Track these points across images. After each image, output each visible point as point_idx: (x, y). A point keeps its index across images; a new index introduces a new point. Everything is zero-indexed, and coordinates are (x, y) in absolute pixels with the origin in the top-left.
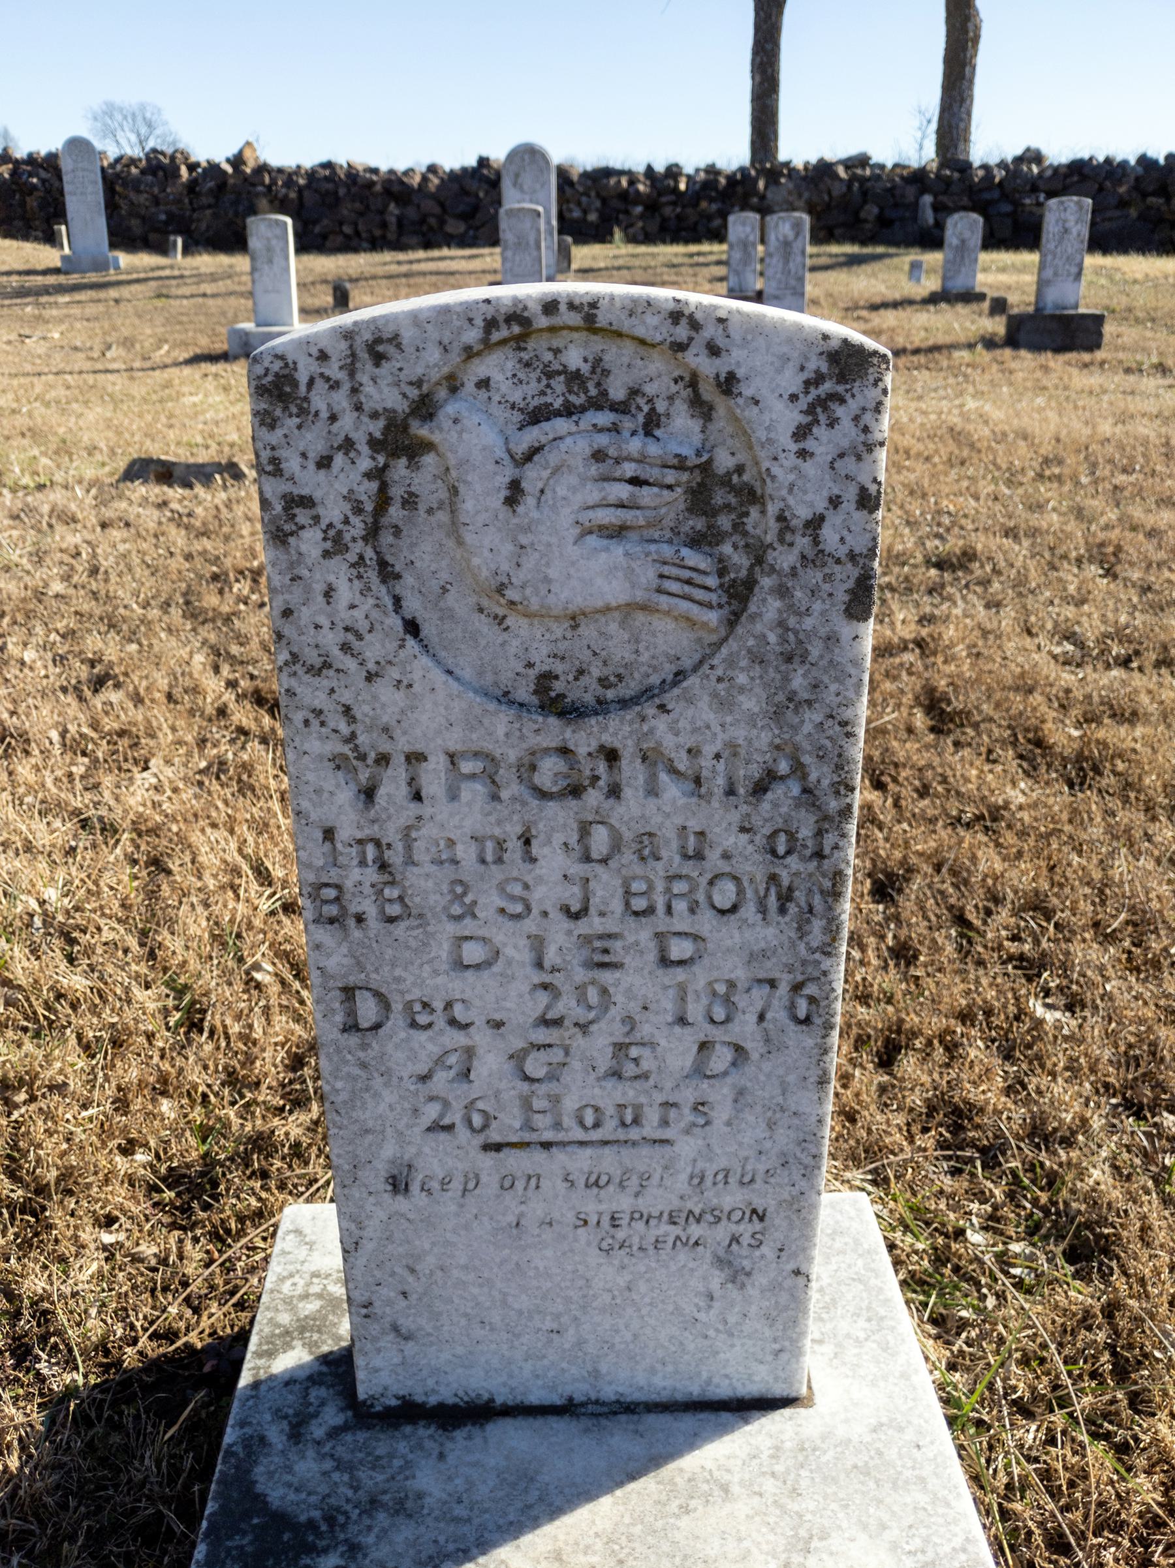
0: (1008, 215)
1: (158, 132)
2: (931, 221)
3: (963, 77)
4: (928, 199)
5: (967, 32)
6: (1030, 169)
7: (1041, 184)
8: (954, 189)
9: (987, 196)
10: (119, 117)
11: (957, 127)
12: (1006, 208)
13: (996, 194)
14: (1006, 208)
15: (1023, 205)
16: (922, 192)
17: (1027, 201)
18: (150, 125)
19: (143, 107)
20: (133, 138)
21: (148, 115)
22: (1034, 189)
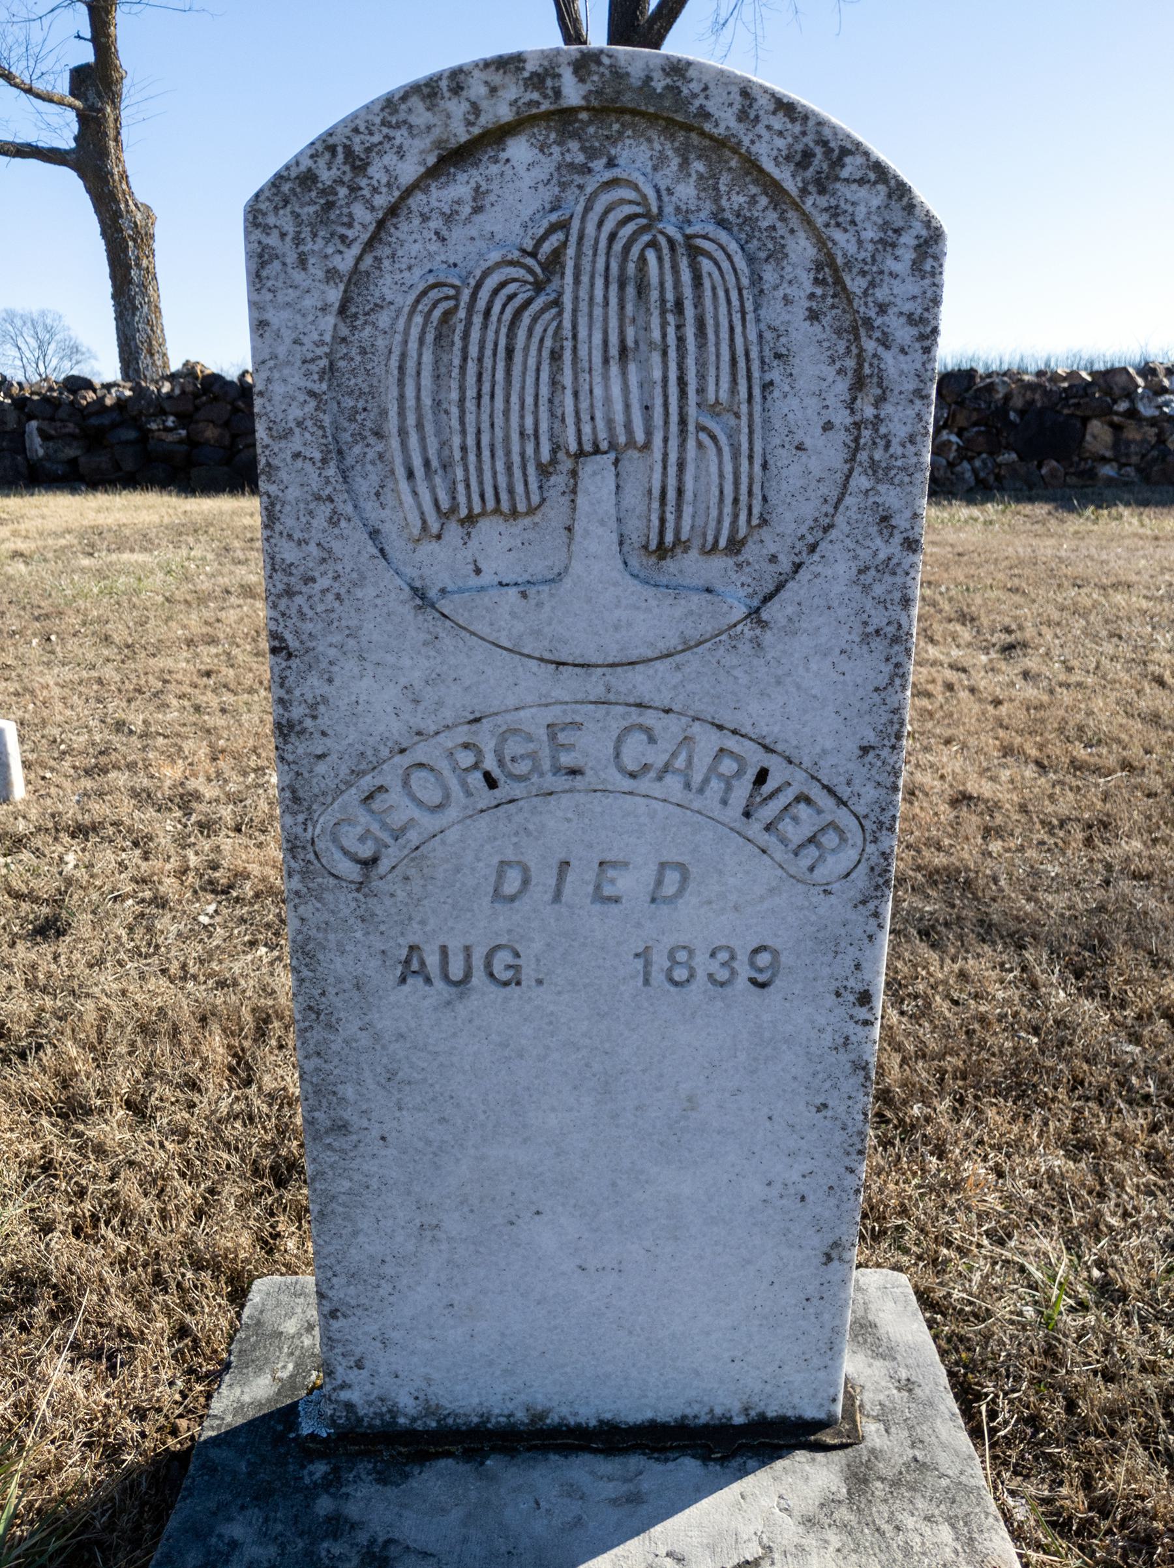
0: (127, 443)
1: (57, 337)
2: (41, 452)
3: (130, 282)
4: (34, 424)
5: (122, 231)
6: (159, 390)
7: (167, 406)
8: (62, 413)
9: (94, 421)
10: (19, 323)
11: (134, 338)
12: (132, 435)
13: (106, 420)
14: (132, 435)
15: (151, 431)
16: (31, 417)
17: (154, 426)
18: (49, 330)
19: (43, 314)
20: (33, 343)
21: (49, 321)
22: (163, 412)
